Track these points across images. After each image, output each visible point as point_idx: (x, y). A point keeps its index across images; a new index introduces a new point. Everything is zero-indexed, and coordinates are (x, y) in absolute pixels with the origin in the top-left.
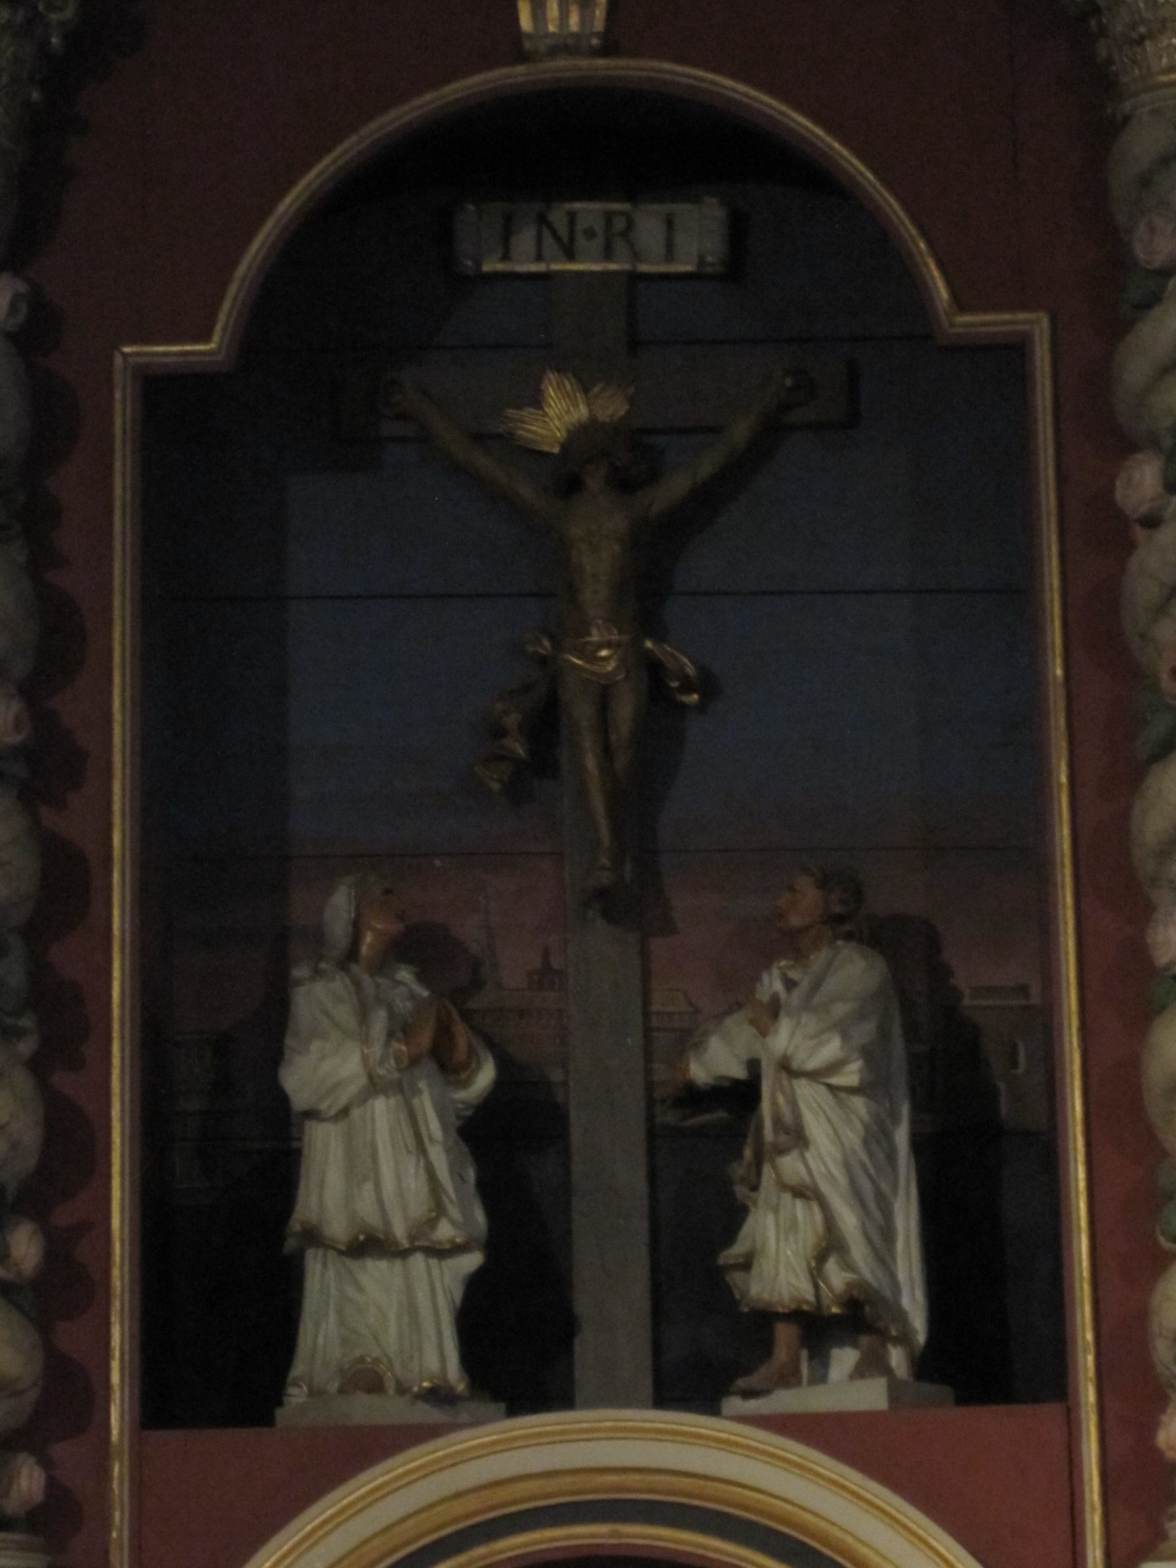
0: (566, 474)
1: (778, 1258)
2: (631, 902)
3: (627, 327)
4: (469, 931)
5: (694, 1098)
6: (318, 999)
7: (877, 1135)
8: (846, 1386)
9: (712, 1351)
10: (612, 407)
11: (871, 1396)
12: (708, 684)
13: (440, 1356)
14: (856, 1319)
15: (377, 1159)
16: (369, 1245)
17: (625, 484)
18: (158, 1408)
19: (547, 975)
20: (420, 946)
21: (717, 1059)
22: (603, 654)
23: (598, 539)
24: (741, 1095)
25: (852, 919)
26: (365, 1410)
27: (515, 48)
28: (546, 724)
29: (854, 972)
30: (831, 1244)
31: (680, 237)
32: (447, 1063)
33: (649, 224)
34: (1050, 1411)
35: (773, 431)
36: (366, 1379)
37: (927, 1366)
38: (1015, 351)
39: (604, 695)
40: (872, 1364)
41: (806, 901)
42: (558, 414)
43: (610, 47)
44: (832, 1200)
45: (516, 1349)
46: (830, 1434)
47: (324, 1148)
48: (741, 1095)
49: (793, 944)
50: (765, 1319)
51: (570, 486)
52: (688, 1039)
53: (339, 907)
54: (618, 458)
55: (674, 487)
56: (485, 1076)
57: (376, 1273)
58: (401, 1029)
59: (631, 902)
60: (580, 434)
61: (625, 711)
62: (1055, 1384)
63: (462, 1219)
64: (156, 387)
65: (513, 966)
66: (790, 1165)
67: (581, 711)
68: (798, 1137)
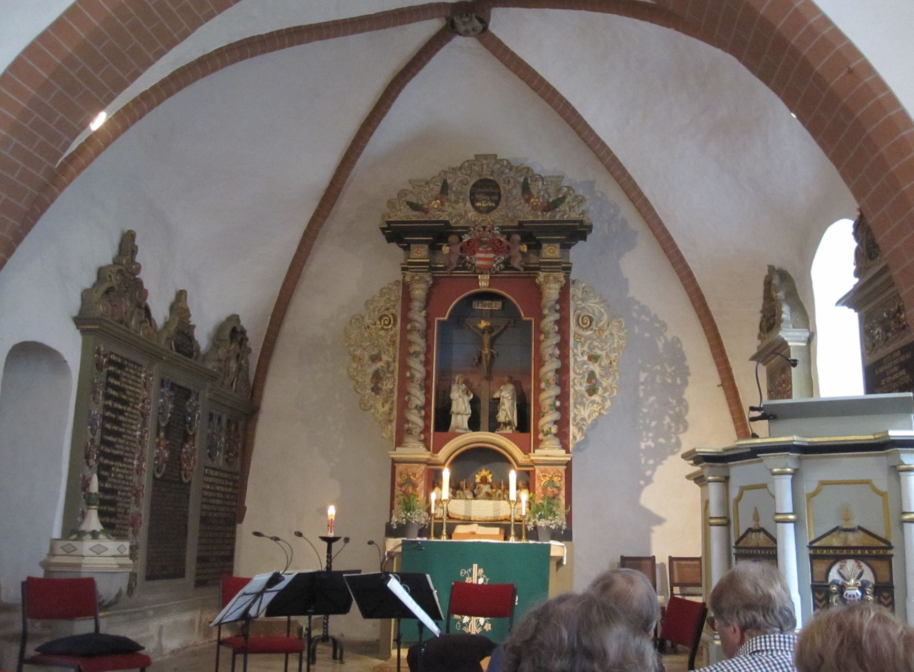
0: (483, 331)
1: (501, 417)
2: (489, 378)
3: (492, 314)
4: (471, 380)
5: (494, 399)
6: (454, 387)
7: (513, 404)
8: (508, 430)
9: (494, 426)
10: (489, 324)
11: (510, 431)
12: (498, 355)
13: (466, 425)
14: (508, 424)
15: (461, 404)
16: (458, 414)
17: (489, 333)
18: (436, 430)
19: (479, 385)
20: (466, 382)
21: (496, 395)
22: (486, 351)
23: (486, 338)
24: (499, 399)
25: (511, 381)
26: (458, 431)
27: (478, 287)
28: (480, 358)
29: (511, 387)
30: (507, 415)
31: (497, 305)
32: (467, 394)
33: (494, 303)
34: (528, 434)
35: (506, 327)
36: (458, 428)
37: (517, 429)
38: (530, 322)
39: (486, 356)
40: (511, 428)
41: (506, 379)
42: (483, 324)
43: (489, 287)
44: (507, 411)
45: (474, 424)
46: (506, 435)
47: (454, 404)
48: (499, 399)
49: (505, 384)
50: (500, 423)
51: (484, 333)
52: (494, 393)
53: (457, 378)
54: (490, 329)
55: (495, 333)
56: (472, 396)
57: (459, 417)
58: (463, 391)
59: (489, 378)
60: (486, 327)
61: (488, 358)
62: (529, 431)
63: (469, 411)
64: (439, 321)
65: (476, 384)
66: (503, 407)
67: (484, 358)
68: (504, 404)
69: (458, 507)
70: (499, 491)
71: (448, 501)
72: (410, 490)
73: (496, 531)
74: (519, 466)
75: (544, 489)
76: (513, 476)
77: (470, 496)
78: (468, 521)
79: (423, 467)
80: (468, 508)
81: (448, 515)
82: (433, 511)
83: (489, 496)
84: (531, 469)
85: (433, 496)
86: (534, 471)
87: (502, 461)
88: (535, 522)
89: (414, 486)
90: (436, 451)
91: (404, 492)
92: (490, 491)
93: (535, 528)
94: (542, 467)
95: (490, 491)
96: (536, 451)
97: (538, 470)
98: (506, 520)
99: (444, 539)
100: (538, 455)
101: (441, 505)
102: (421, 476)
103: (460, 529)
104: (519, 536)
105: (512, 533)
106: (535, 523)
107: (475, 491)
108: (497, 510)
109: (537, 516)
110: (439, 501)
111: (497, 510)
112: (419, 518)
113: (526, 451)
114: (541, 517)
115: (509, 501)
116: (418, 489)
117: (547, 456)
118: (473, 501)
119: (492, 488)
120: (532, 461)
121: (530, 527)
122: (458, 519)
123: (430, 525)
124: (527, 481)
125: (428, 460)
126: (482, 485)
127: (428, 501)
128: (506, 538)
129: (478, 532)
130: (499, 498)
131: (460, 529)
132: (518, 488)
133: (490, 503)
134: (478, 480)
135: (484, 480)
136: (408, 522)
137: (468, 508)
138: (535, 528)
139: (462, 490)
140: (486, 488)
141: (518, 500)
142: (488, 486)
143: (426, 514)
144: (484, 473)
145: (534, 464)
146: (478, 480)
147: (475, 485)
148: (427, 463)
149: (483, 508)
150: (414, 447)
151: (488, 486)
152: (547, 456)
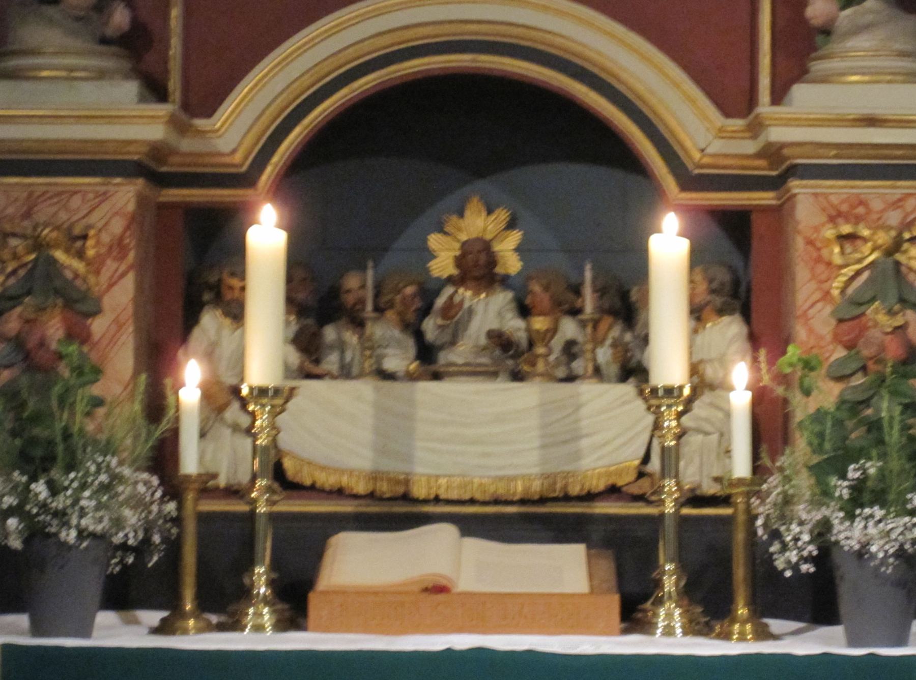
69: (338, 428)
70: (569, 328)
71: (276, 397)
72: (54, 329)
73: (566, 567)
74: (691, 181)
75: (850, 318)
76: (669, 247)
77: (399, 358)
78: (395, 510)
79: (126, 194)
80: (393, 429)
81: (278, 473)
82: (190, 463)
83: (510, 358)
84: (765, 198)
85: (191, 381)
86: (780, 214)
87: (596, 159)
88: (822, 530)
89: (79, 305)
90: (204, 98)
91: (18, 342)
92: (515, 326)
93: (826, 552)
94: (839, 190)
95: (515, 326)
96: (801, 92)
97: (808, 201)
98: (613, 491)
99: (259, 634)
100: (812, 114)
101: (233, 412)
102: (118, 248)
103: (356, 562)
104: (709, 605)
105: (669, 584)
106: (822, 530)
107: (430, 327)
108: (561, 435)
109: (842, 489)
110: (223, 396)
111: (561, 435)
112: (108, 505)
113: (734, 97)
114: (861, 496)
115: (656, 398)
116: (98, 326)
117: (871, 121)
118: (427, 389)
119: (524, 311)
120: (773, 153)
121: (793, 556)
122: (339, 493)
123: (174, 548)
124: (743, 274)
125: (158, 151)
126: (465, 294)
127: (157, 406)
128: (634, 614)
129: (466, 582)
130: (569, 367)
131: (356, 562)
132: (697, 313)
133: (526, 396)
134: (443, 264)
135: (478, 268)
136: (36, 534)
137: (393, 429)
138: (826, 552)
139: (358, 324)
140: (491, 311)
141: (703, 382)
142: (502, 299)
143: (145, 484)
144: (477, 223)
145: (782, 170)
146: (443, 264)
147: (428, 293)
148: (152, 168)
149: (484, 429)
150: (71, 77)
151: (502, 299)
152: (871, 121)
